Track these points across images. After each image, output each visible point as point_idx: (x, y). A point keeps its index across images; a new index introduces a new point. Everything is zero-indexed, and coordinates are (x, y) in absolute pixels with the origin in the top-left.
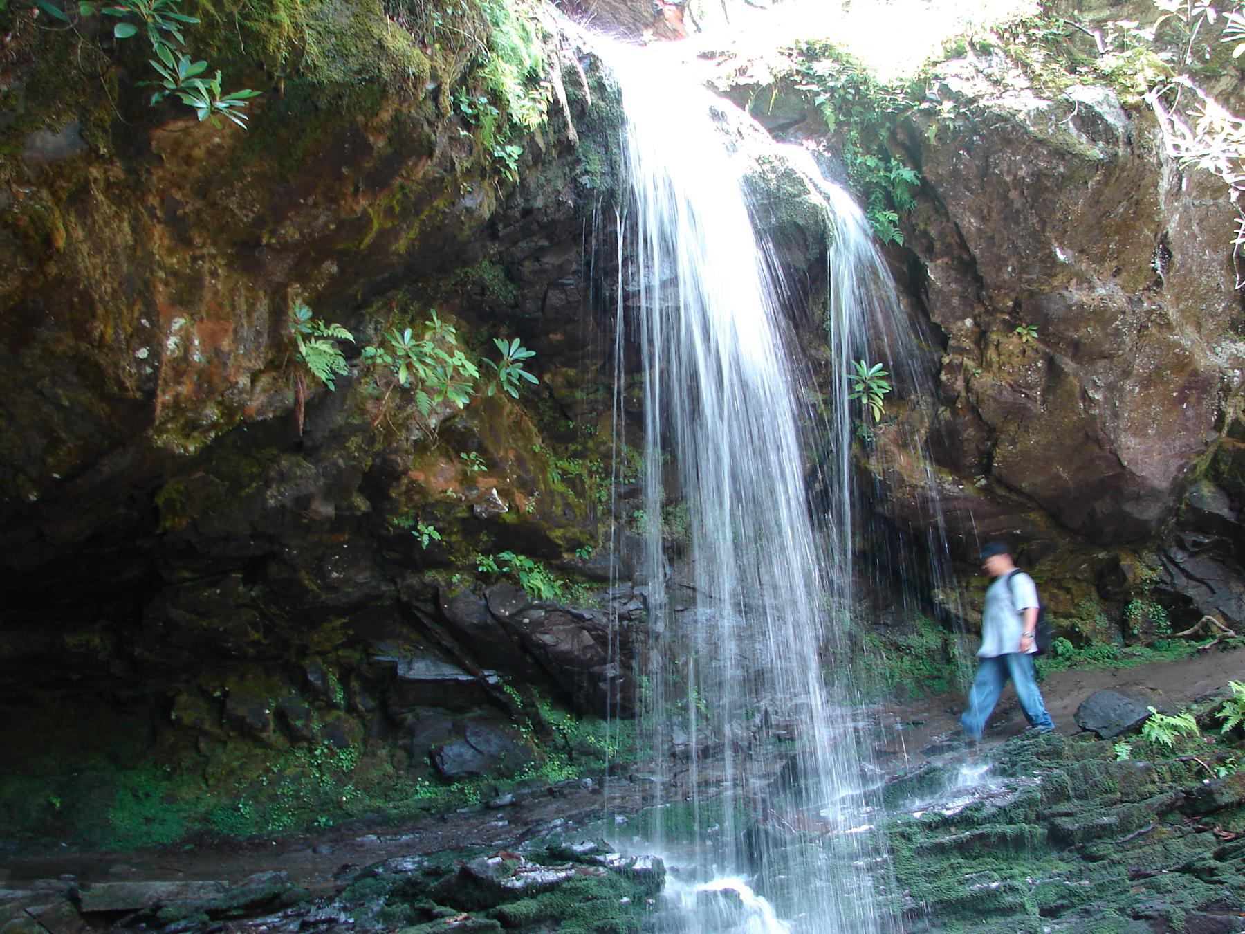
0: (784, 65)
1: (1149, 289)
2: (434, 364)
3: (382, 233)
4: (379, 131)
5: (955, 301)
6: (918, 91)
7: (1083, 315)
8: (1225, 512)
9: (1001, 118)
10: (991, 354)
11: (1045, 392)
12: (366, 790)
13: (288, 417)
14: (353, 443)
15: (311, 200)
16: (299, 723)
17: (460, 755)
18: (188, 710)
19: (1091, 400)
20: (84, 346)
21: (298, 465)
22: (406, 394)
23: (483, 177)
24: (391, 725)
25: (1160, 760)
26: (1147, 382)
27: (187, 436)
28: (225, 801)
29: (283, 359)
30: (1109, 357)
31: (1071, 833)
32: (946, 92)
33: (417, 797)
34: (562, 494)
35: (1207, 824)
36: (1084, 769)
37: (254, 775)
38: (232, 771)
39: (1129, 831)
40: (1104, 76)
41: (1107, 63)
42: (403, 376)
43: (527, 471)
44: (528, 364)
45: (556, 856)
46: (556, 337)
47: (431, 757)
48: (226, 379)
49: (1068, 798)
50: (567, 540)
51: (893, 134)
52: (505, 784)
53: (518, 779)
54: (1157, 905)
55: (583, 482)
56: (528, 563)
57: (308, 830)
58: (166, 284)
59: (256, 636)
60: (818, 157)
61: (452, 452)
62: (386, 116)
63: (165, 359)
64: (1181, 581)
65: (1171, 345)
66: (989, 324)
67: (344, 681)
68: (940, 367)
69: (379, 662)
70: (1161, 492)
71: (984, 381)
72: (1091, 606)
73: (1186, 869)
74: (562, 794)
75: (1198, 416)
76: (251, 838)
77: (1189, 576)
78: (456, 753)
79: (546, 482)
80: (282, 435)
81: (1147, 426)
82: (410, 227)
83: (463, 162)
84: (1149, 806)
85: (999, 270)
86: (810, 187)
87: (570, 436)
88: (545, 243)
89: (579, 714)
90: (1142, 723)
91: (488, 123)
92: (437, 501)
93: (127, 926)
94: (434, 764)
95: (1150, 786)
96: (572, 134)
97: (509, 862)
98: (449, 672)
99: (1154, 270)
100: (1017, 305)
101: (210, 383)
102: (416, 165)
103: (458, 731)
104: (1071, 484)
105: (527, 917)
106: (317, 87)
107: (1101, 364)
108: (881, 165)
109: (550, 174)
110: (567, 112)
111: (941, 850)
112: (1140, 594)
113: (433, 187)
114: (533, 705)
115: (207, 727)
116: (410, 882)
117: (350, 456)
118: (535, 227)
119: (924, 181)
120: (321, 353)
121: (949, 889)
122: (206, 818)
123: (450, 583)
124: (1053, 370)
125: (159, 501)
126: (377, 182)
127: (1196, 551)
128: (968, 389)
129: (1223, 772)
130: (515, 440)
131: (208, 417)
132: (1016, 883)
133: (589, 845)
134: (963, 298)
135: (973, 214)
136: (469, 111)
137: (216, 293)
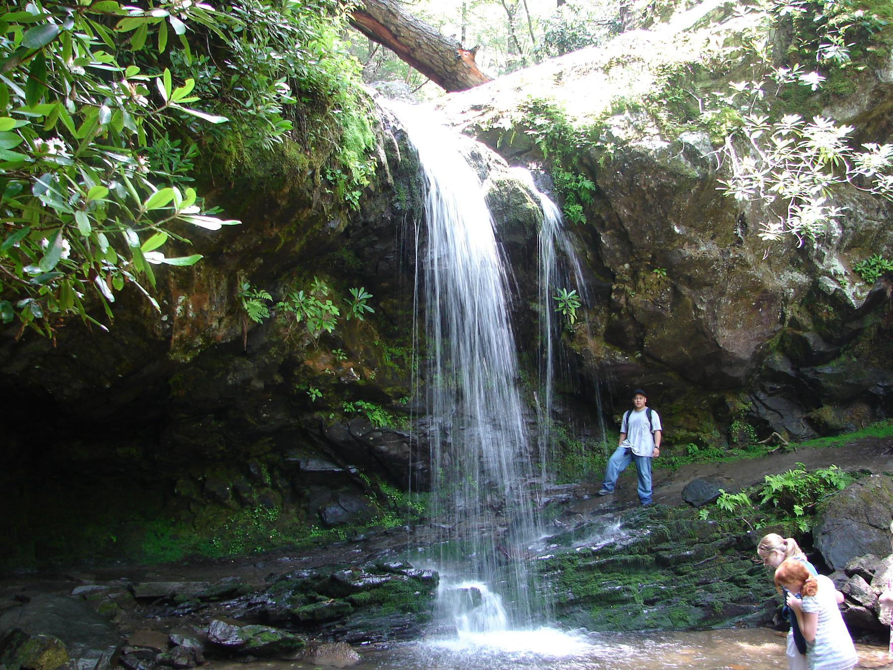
0: (519, 117)
1: (734, 245)
2: (316, 308)
3: (286, 243)
4: (283, 198)
5: (618, 255)
6: (596, 133)
7: (692, 263)
8: (789, 370)
9: (639, 154)
10: (641, 284)
11: (672, 305)
12: (283, 532)
13: (238, 340)
14: (273, 350)
15: (248, 231)
16: (246, 495)
17: (335, 512)
18: (184, 488)
19: (699, 310)
20: (136, 317)
21: (245, 363)
22: (303, 324)
23: (340, 210)
24: (296, 496)
25: (724, 519)
26: (735, 297)
27: (186, 353)
28: (206, 538)
29: (235, 309)
30: (711, 285)
31: (667, 560)
32: (610, 134)
33: (311, 536)
34: (391, 368)
35: (748, 555)
36: (677, 524)
37: (221, 524)
38: (209, 521)
39: (702, 559)
40: (703, 125)
41: (707, 116)
42: (299, 318)
43: (370, 356)
44: (369, 302)
45: (381, 570)
46: (385, 285)
47: (319, 512)
48: (206, 325)
49: (668, 541)
50: (395, 393)
51: (581, 161)
52: (360, 529)
53: (368, 526)
54: (708, 599)
55: (403, 360)
56: (373, 407)
57: (251, 554)
58: (175, 278)
59: (221, 448)
60: (536, 175)
61: (328, 349)
62: (287, 190)
63: (175, 319)
64: (763, 411)
65: (749, 277)
66: (638, 267)
67: (270, 471)
68: (611, 291)
69: (290, 461)
70: (745, 361)
71: (637, 299)
72: (710, 425)
73: (731, 580)
74: (392, 534)
75: (769, 316)
76: (220, 559)
77: (768, 408)
78: (333, 511)
79: (382, 362)
80: (236, 348)
81: (737, 322)
82: (301, 239)
83: (327, 206)
84: (714, 546)
85: (642, 238)
86: (528, 198)
87: (396, 335)
88: (376, 239)
89: (403, 489)
90: (717, 497)
91: (341, 183)
92: (320, 376)
93: (158, 605)
94: (321, 518)
95: (716, 534)
96: (390, 180)
97: (356, 573)
98: (328, 466)
99: (737, 235)
100: (654, 256)
101: (198, 328)
102: (303, 212)
103: (335, 499)
104: (690, 357)
105: (365, 601)
106: (251, 180)
107: (705, 289)
108: (574, 178)
109: (378, 202)
110: (387, 168)
111: (590, 568)
112: (739, 418)
113: (313, 220)
114: (377, 485)
115: (194, 497)
116: (305, 583)
117: (272, 357)
118: (370, 231)
119: (597, 187)
120: (254, 307)
121: (592, 590)
122: (195, 547)
123: (328, 418)
124: (677, 294)
125: (171, 382)
126: (283, 220)
127: (772, 393)
128: (627, 303)
129: (758, 526)
130: (364, 340)
131: (197, 343)
132: (630, 587)
133: (397, 565)
134: (622, 253)
135: (626, 207)
136: (331, 178)
137: (200, 279)
